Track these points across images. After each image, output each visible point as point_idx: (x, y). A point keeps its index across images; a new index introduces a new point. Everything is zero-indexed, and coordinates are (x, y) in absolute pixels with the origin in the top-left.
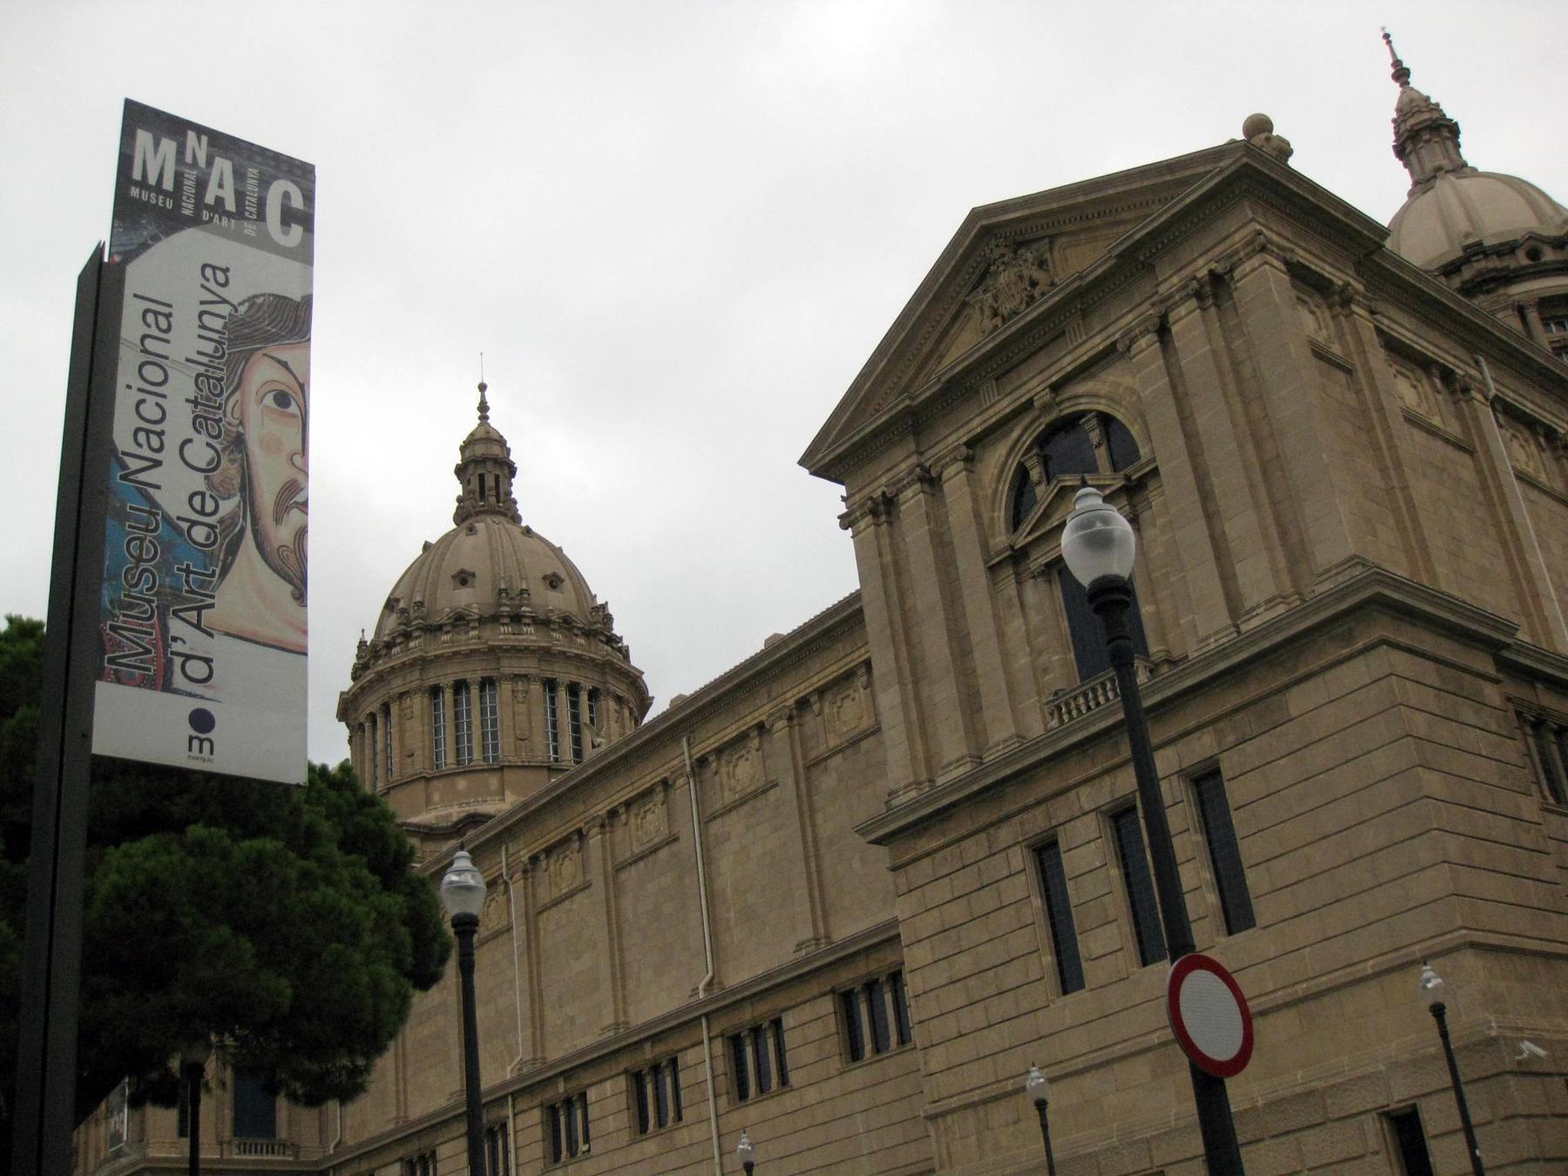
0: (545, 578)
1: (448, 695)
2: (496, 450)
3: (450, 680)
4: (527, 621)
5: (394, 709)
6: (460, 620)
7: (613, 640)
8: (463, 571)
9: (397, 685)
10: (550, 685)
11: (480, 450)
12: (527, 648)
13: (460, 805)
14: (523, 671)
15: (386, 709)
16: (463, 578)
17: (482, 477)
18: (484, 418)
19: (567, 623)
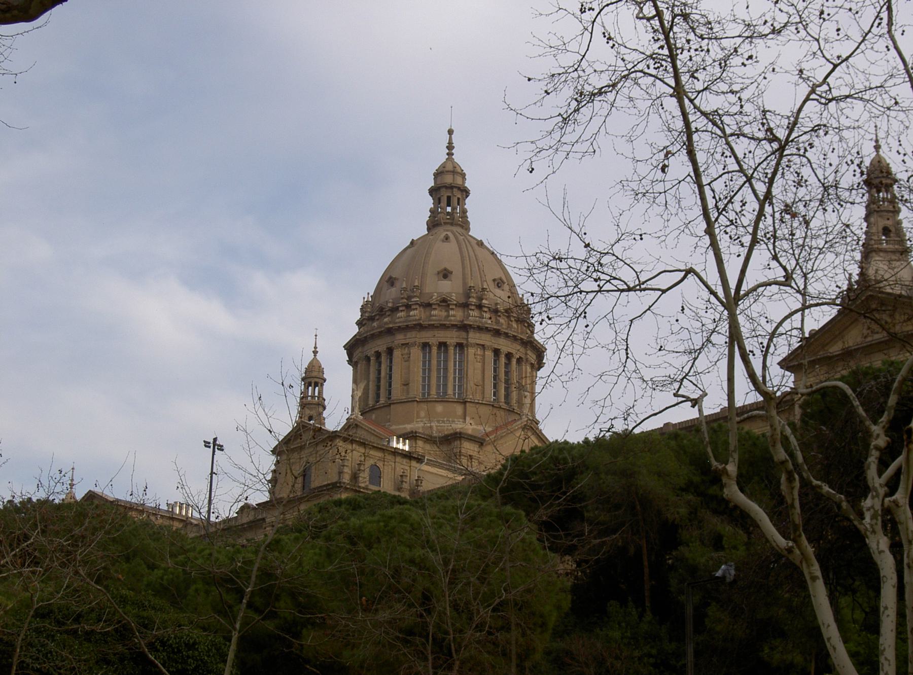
0: (494, 280)
1: (435, 350)
2: (459, 181)
4: (486, 309)
5: (397, 353)
6: (445, 302)
8: (445, 269)
9: (400, 338)
10: (497, 352)
11: (448, 179)
12: (487, 328)
13: (438, 421)
14: (482, 342)
15: (390, 351)
16: (446, 274)
17: (449, 198)
18: (450, 154)
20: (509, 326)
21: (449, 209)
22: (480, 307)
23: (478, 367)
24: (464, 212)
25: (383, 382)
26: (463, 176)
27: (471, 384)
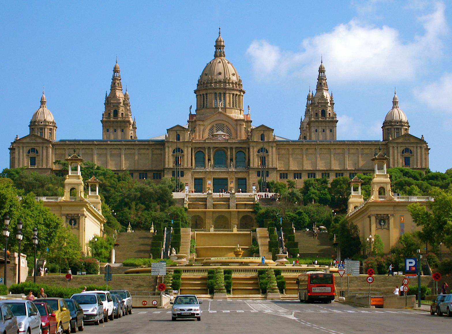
0: (232, 74)
1: (218, 94)
2: (222, 43)
3: (218, 92)
5: (208, 95)
6: (220, 82)
7: (241, 85)
8: (220, 72)
9: (209, 91)
10: (233, 94)
11: (219, 44)
15: (207, 94)
16: (220, 74)
18: (220, 35)
19: (236, 83)
20: (236, 87)
21: (220, 50)
22: (229, 83)
23: (229, 99)
24: (224, 52)
25: (205, 102)
26: (223, 42)
27: (227, 104)
